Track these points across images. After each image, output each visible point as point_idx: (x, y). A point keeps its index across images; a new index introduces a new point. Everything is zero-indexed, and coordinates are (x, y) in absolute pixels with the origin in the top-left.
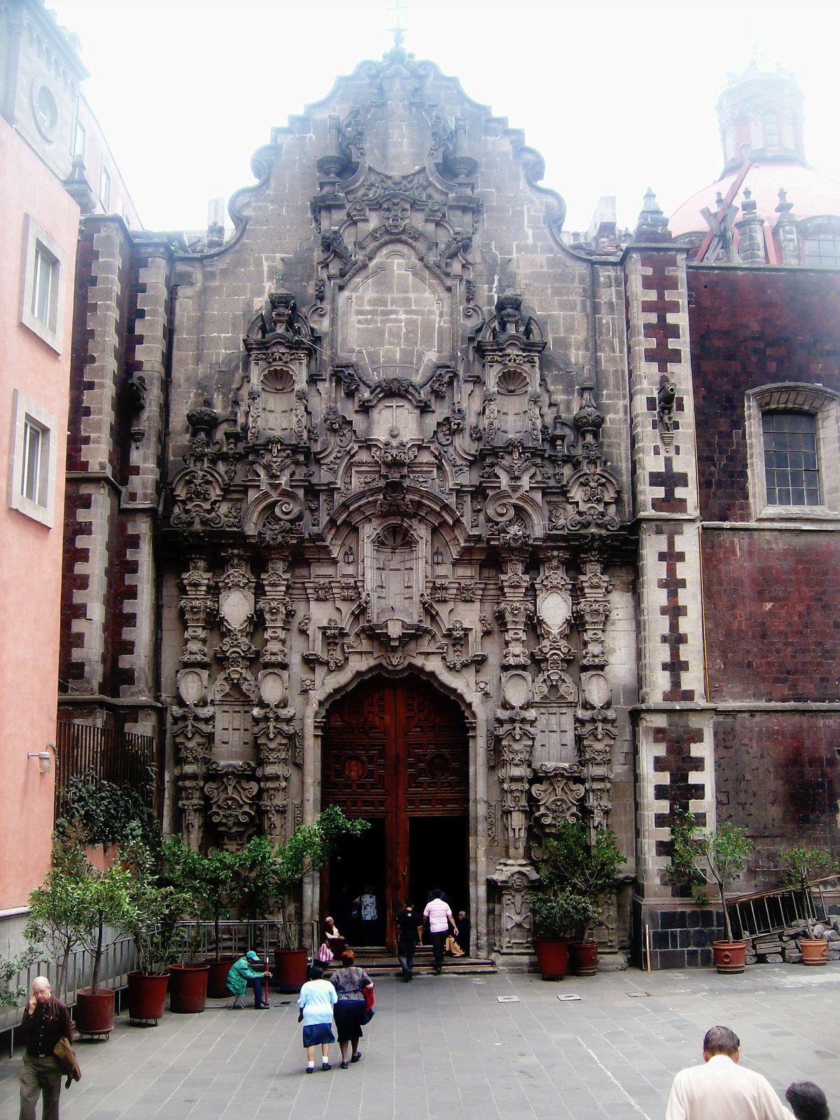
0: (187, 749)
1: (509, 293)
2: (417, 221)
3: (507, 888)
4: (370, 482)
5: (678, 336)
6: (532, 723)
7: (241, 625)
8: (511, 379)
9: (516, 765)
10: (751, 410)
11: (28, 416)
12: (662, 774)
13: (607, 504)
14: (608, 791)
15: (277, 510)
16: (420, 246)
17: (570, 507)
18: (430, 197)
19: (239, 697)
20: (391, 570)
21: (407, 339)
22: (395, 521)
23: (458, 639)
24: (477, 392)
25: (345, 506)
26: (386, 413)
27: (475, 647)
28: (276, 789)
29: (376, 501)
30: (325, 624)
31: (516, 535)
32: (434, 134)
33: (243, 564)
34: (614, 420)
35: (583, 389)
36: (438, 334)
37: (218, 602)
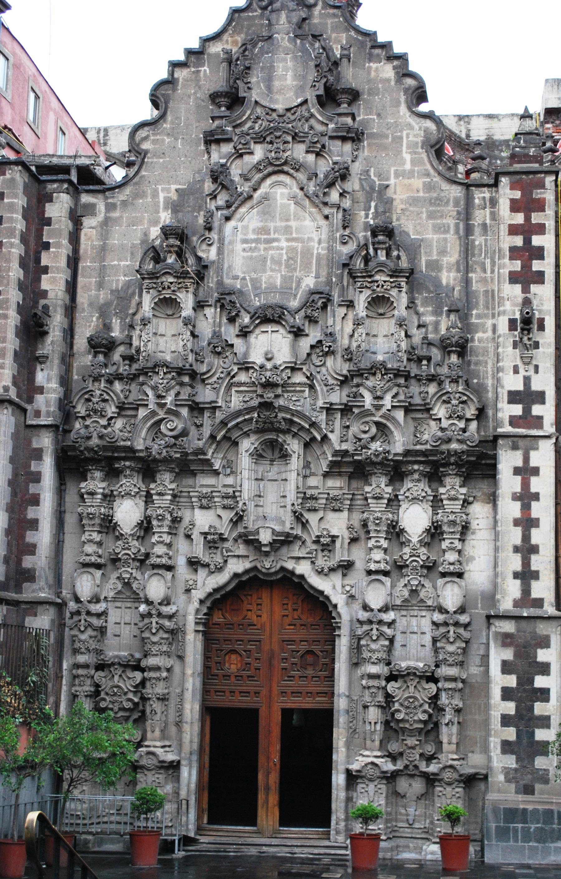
0: (80, 641)
3: (362, 777)
4: (248, 401)
5: (542, 257)
6: (390, 624)
7: (132, 530)
9: (373, 663)
12: (508, 677)
13: (468, 420)
14: (460, 690)
15: (162, 427)
16: (301, 176)
17: (433, 423)
18: (311, 128)
20: (269, 480)
21: (288, 266)
22: (272, 436)
24: (350, 316)
25: (224, 423)
26: (262, 337)
28: (158, 679)
29: (252, 419)
30: (206, 530)
31: (376, 451)
32: (317, 66)
33: (135, 474)
35: (450, 311)
36: (317, 261)
37: (112, 508)
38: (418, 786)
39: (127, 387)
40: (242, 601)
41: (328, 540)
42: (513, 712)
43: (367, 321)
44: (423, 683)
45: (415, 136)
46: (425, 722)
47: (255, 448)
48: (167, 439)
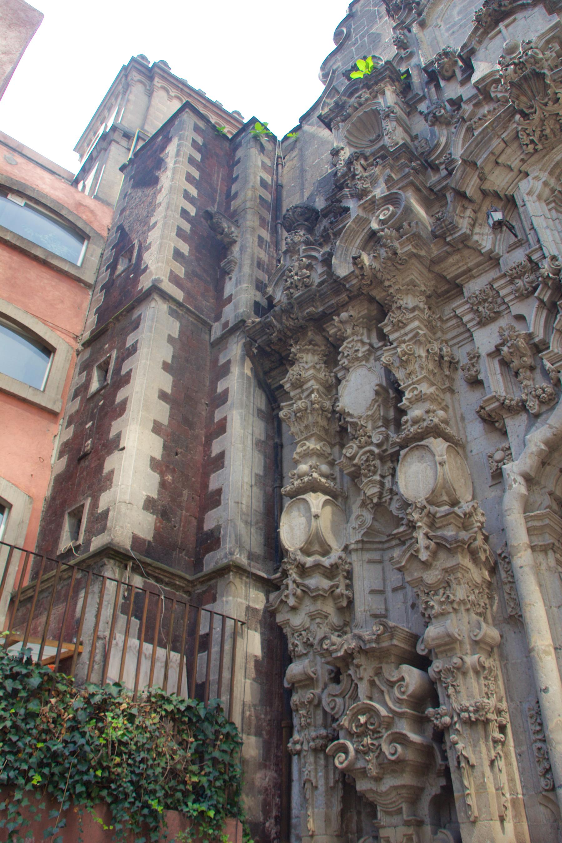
7: (369, 409)
47: (545, 184)
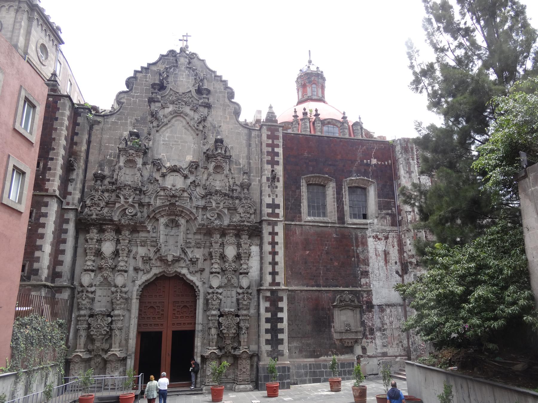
1: (219, 137)
2: (187, 110)
5: (278, 156)
6: (221, 294)
8: (218, 168)
10: (303, 183)
11: (14, 166)
13: (251, 214)
14: (248, 320)
15: (127, 211)
17: (237, 215)
18: (192, 101)
19: (107, 283)
22: (173, 217)
23: (193, 262)
24: (206, 172)
25: (154, 211)
26: (172, 178)
27: (200, 265)
29: (166, 210)
30: (144, 255)
33: (112, 231)
34: (255, 184)
35: (244, 173)
38: (231, 360)
39: (111, 195)
40: (157, 285)
41: (196, 260)
42: (269, 328)
43: (213, 175)
44: (234, 317)
45: (231, 109)
46: (234, 334)
48: (128, 216)
